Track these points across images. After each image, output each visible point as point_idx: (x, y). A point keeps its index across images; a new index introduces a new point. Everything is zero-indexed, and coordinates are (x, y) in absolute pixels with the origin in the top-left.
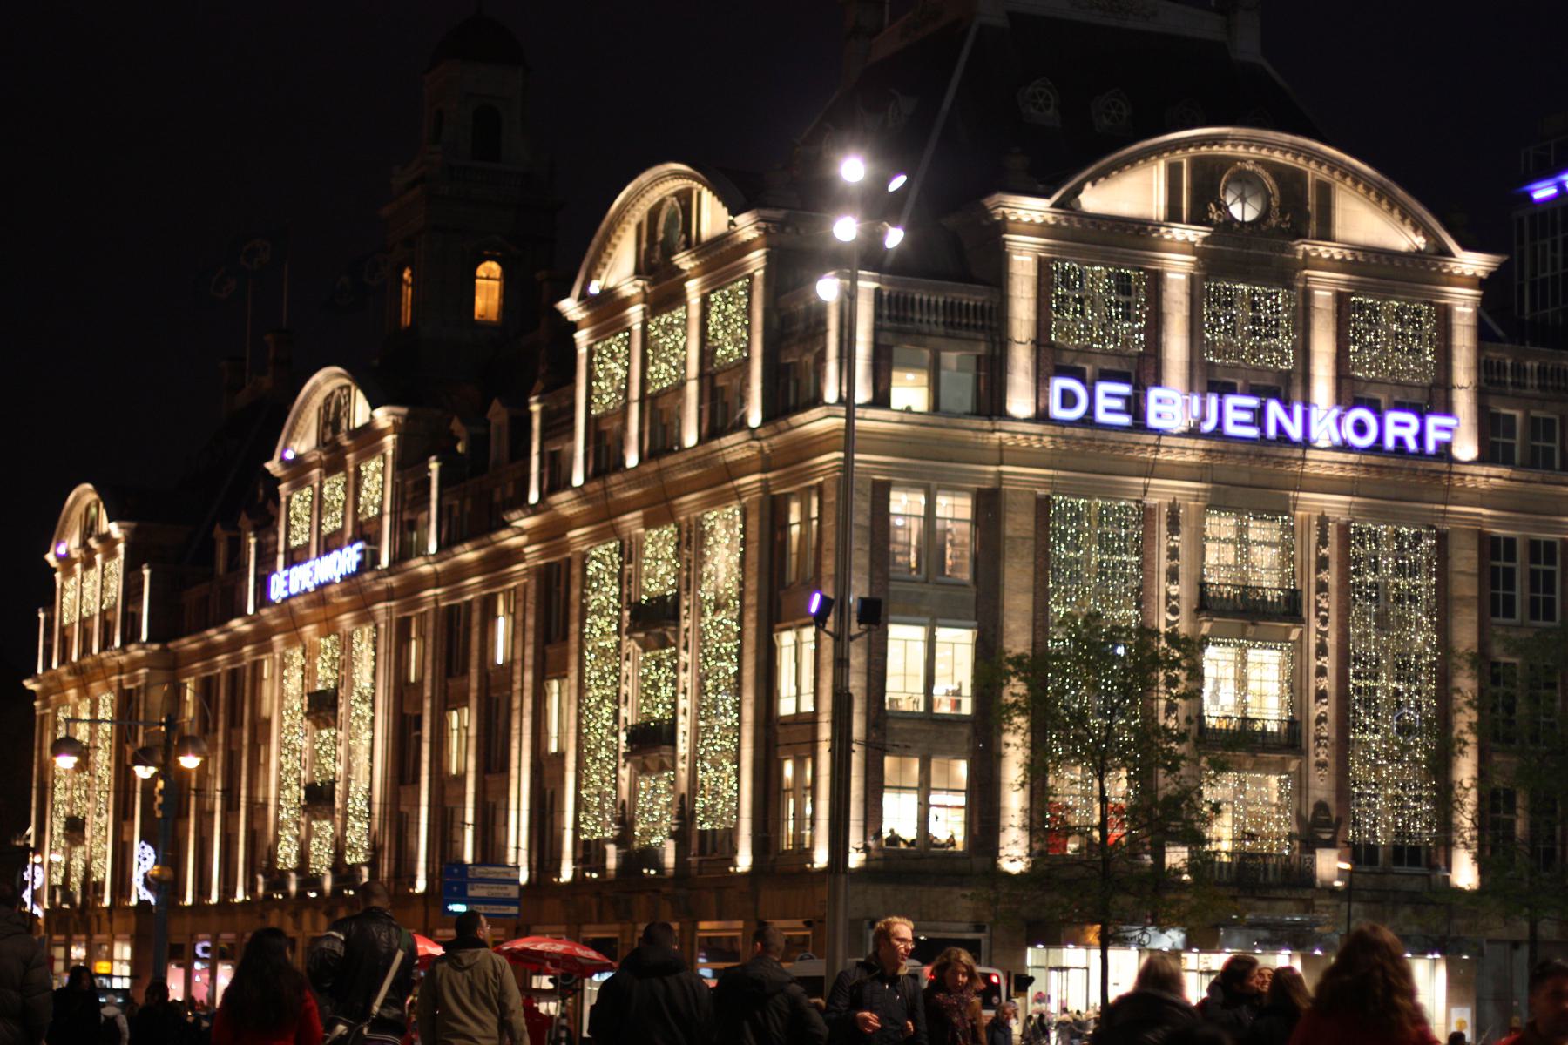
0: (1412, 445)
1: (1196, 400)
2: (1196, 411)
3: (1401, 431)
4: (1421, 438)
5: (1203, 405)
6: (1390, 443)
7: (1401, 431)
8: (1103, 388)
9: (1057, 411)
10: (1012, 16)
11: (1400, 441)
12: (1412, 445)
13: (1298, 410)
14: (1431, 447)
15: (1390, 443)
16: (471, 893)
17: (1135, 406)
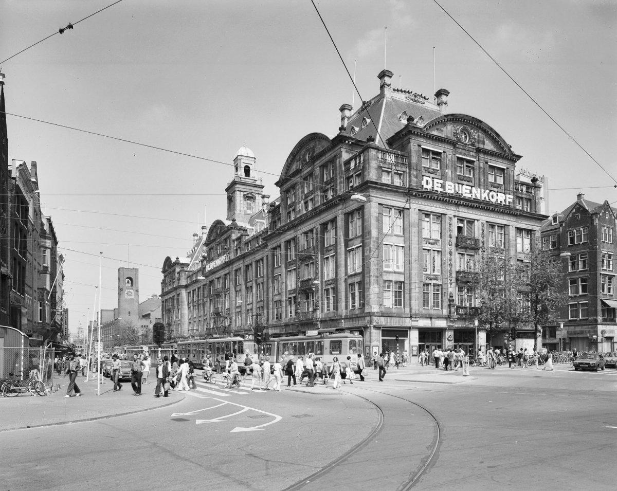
4: (505, 201)
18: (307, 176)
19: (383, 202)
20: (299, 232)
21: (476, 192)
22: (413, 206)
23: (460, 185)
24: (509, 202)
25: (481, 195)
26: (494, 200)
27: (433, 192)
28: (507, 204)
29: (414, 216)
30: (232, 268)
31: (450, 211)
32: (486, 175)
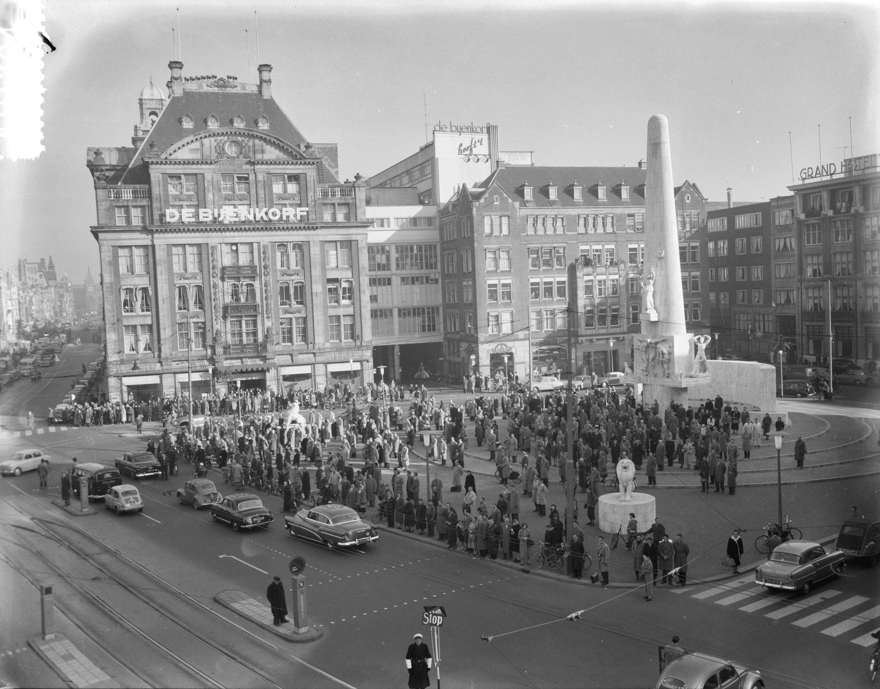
0: (292, 218)
1: (216, 211)
2: (216, 215)
4: (295, 215)
6: (284, 218)
7: (287, 214)
9: (168, 219)
11: (288, 217)
14: (299, 218)
15: (284, 218)
19: (119, 243)
24: (301, 216)
25: (255, 218)
31: (213, 239)
32: (268, 186)
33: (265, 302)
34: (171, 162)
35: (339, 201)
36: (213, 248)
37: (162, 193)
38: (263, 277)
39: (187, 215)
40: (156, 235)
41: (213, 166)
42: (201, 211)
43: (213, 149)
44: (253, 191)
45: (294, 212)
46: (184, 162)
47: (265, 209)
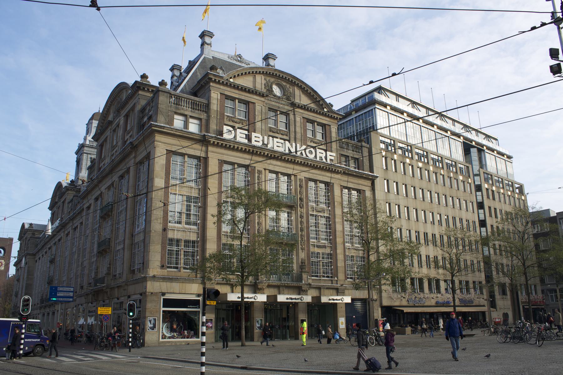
3: (321, 155)
5: (268, 139)
6: (318, 159)
7: (321, 155)
8: (239, 131)
9: (226, 136)
10: (212, 57)
11: (321, 158)
12: (324, 160)
13: (294, 144)
14: (329, 161)
16: (58, 295)
17: (249, 138)
18: (116, 128)
20: (103, 188)
21: (290, 146)
22: (210, 155)
23: (271, 138)
26: (311, 157)
27: (234, 141)
28: (329, 161)
29: (213, 167)
30: (64, 232)
33: (300, 233)
34: (231, 84)
35: (352, 156)
36: (260, 172)
37: (219, 110)
38: (299, 208)
39: (241, 136)
40: (210, 148)
41: (263, 99)
42: (254, 135)
43: (263, 86)
44: (292, 129)
45: (324, 155)
46: (242, 88)
47: (304, 147)
